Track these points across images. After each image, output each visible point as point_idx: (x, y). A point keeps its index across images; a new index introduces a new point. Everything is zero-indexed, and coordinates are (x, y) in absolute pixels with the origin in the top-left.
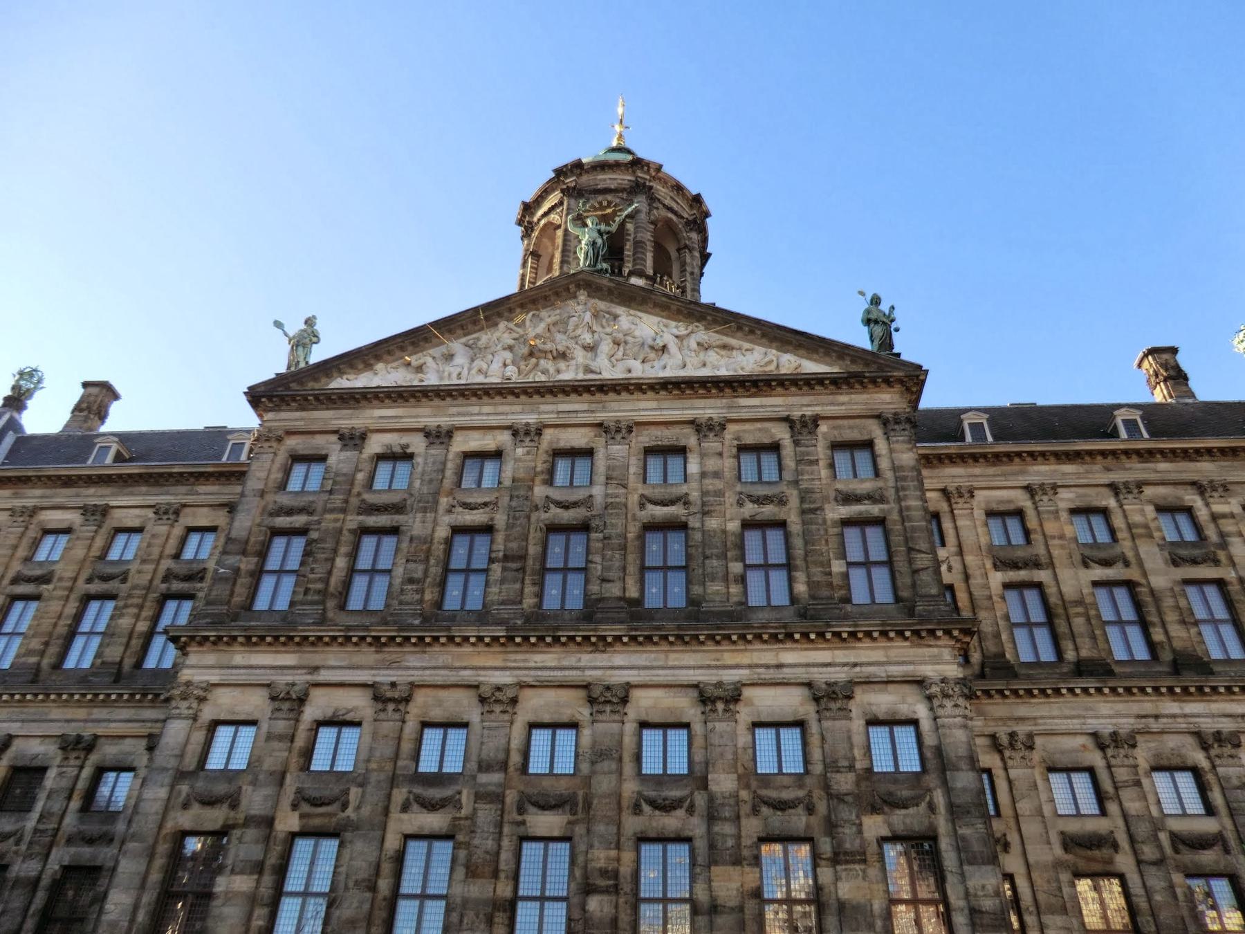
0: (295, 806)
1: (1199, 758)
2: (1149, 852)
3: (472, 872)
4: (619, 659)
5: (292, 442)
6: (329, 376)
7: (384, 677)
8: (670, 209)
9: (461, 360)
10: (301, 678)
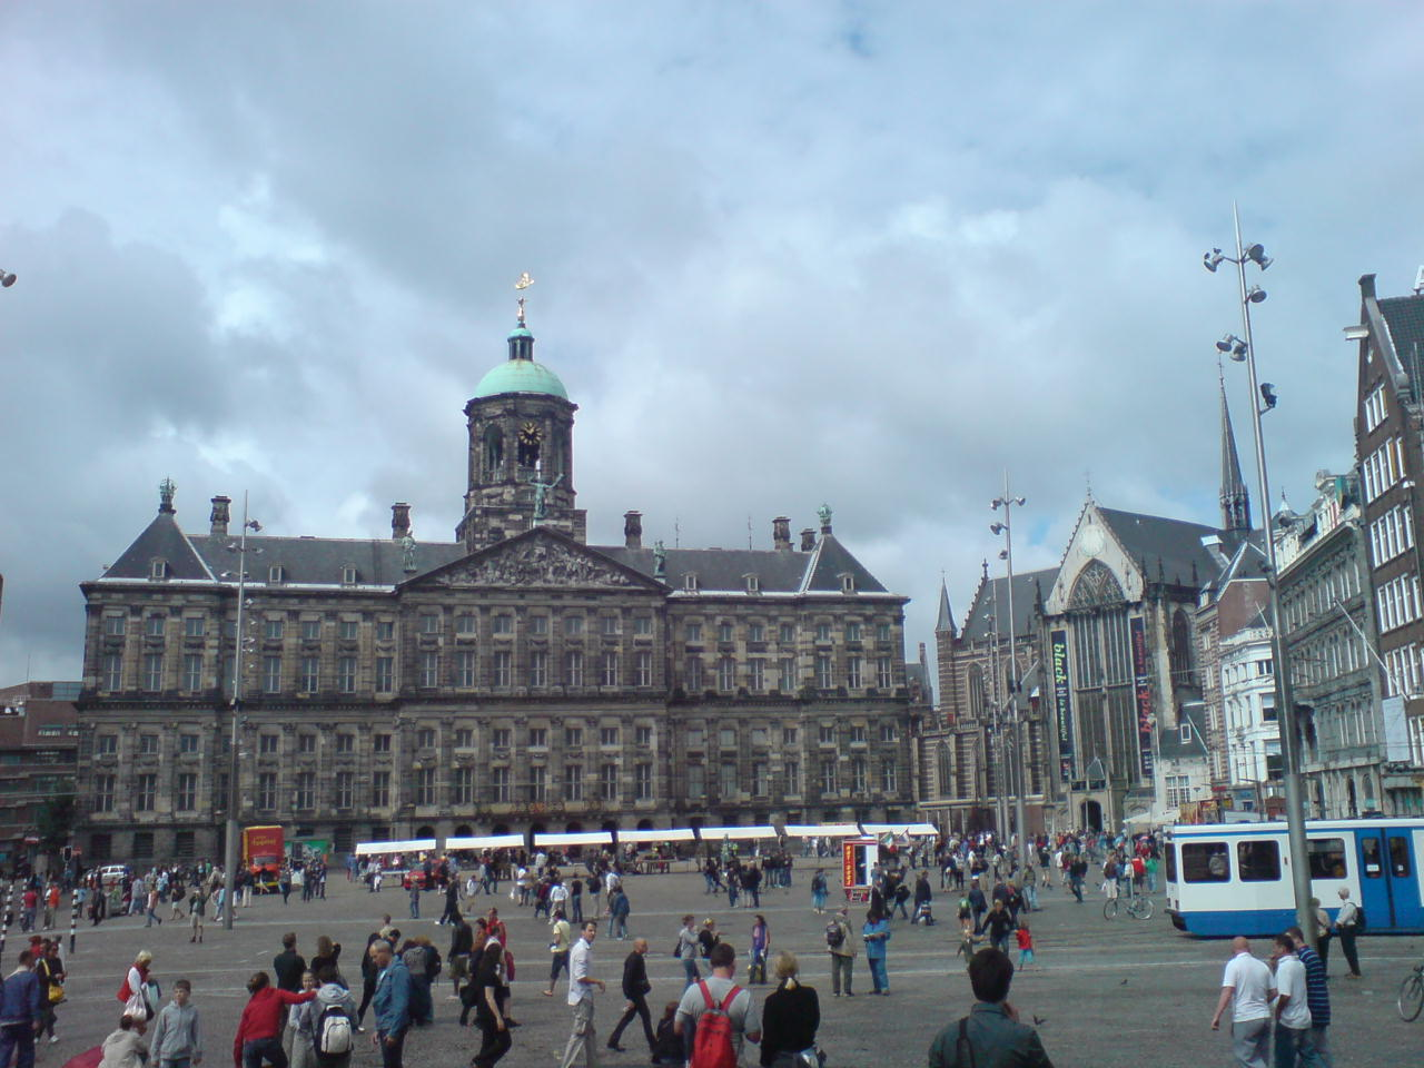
0: (457, 760)
1: (737, 728)
2: (713, 757)
3: (518, 778)
4: (559, 707)
5: (421, 608)
7: (479, 714)
8: (562, 422)
10: (451, 716)
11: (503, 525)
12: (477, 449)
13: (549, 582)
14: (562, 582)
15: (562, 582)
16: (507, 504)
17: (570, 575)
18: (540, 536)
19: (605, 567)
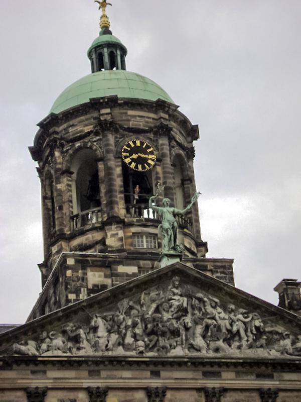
6: (8, 341)
8: (180, 145)
9: (102, 332)
11: (108, 281)
12: (59, 186)
13: (199, 350)
14: (217, 350)
15: (217, 350)
16: (112, 252)
17: (228, 341)
18: (176, 279)
19: (280, 329)
